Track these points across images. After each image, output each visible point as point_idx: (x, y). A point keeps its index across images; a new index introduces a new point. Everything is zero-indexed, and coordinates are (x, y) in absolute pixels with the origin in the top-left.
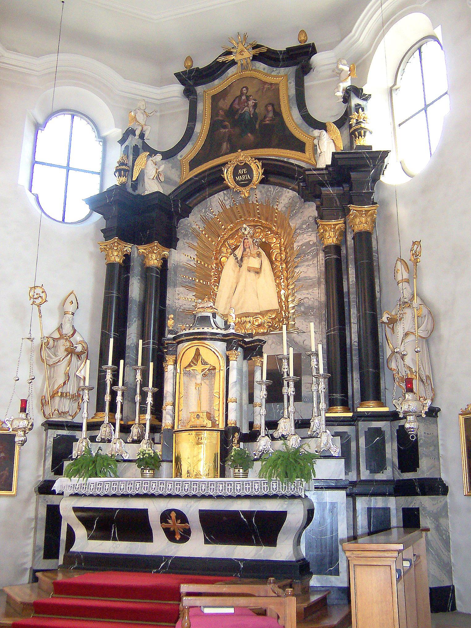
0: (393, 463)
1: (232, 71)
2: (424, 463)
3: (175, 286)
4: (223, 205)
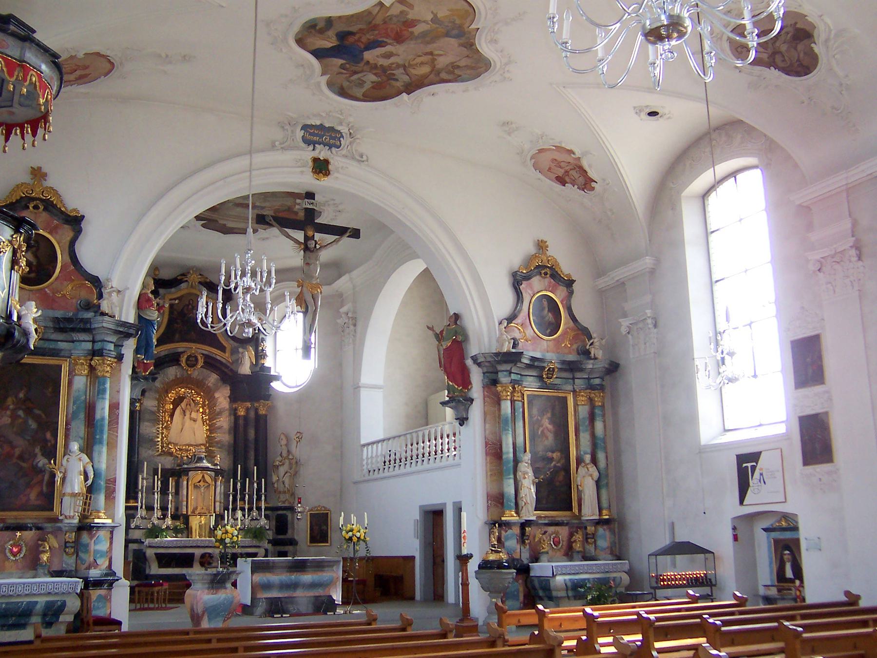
1: (183, 285)
2: (290, 531)
4: (176, 376)
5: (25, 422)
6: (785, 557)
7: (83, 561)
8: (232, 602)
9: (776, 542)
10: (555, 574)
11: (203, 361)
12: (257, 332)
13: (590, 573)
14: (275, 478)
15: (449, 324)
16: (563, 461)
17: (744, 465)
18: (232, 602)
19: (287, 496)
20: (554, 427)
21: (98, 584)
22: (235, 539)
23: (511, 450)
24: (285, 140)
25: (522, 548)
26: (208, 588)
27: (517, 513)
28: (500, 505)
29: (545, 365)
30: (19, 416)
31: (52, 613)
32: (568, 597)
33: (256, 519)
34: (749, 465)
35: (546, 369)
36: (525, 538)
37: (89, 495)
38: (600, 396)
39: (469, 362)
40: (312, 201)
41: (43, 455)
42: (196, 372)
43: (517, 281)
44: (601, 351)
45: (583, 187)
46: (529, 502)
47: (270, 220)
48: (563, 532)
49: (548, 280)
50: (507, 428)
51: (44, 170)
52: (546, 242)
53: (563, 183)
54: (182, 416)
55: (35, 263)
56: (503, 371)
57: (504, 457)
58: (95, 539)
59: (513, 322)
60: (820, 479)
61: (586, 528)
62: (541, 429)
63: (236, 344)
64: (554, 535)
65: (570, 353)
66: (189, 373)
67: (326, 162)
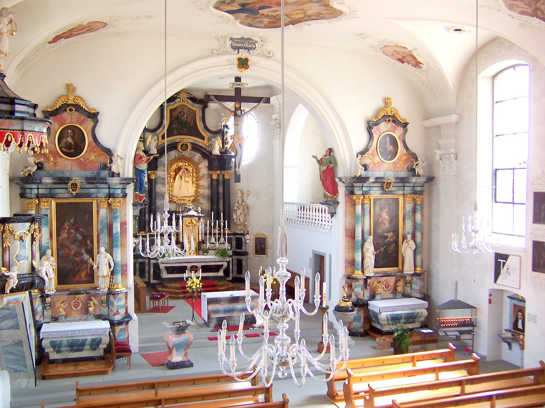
0: (234, 247)
1: (178, 100)
2: (244, 248)
3: (157, 184)
4: (175, 156)
5: (76, 236)
6: (519, 316)
7: (112, 311)
8: (188, 341)
9: (515, 306)
10: (381, 312)
11: (191, 146)
12: (223, 128)
13: (403, 310)
14: (235, 217)
15: (326, 155)
16: (394, 237)
17: (499, 260)
18: (188, 341)
19: (242, 227)
20: (389, 217)
21: (120, 323)
22: (198, 286)
23: (361, 235)
24: (220, 47)
25: (365, 291)
26: (176, 334)
27: (363, 272)
28: (352, 266)
29: (385, 181)
30: (72, 233)
31: (95, 344)
32: (389, 324)
33: (223, 243)
34: (502, 261)
35: (386, 183)
36: (367, 285)
37: (112, 276)
38: (420, 198)
39: (337, 180)
40: (239, 83)
41: (86, 253)
42: (188, 153)
43: (369, 128)
44: (422, 170)
45: (415, 65)
46: (370, 266)
47: (213, 99)
48: (391, 281)
49: (391, 123)
50: (358, 222)
51: (75, 85)
52: (391, 99)
53: (403, 62)
54: (180, 180)
55: (73, 144)
56: (357, 187)
57: (356, 239)
58: (117, 299)
59: (366, 153)
60: (541, 282)
61: (406, 278)
62: (381, 219)
63: (211, 135)
64: (386, 282)
65: (403, 171)
66: (183, 154)
67: (247, 60)
